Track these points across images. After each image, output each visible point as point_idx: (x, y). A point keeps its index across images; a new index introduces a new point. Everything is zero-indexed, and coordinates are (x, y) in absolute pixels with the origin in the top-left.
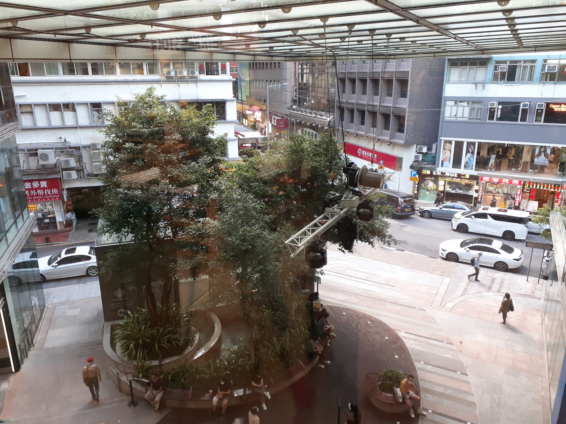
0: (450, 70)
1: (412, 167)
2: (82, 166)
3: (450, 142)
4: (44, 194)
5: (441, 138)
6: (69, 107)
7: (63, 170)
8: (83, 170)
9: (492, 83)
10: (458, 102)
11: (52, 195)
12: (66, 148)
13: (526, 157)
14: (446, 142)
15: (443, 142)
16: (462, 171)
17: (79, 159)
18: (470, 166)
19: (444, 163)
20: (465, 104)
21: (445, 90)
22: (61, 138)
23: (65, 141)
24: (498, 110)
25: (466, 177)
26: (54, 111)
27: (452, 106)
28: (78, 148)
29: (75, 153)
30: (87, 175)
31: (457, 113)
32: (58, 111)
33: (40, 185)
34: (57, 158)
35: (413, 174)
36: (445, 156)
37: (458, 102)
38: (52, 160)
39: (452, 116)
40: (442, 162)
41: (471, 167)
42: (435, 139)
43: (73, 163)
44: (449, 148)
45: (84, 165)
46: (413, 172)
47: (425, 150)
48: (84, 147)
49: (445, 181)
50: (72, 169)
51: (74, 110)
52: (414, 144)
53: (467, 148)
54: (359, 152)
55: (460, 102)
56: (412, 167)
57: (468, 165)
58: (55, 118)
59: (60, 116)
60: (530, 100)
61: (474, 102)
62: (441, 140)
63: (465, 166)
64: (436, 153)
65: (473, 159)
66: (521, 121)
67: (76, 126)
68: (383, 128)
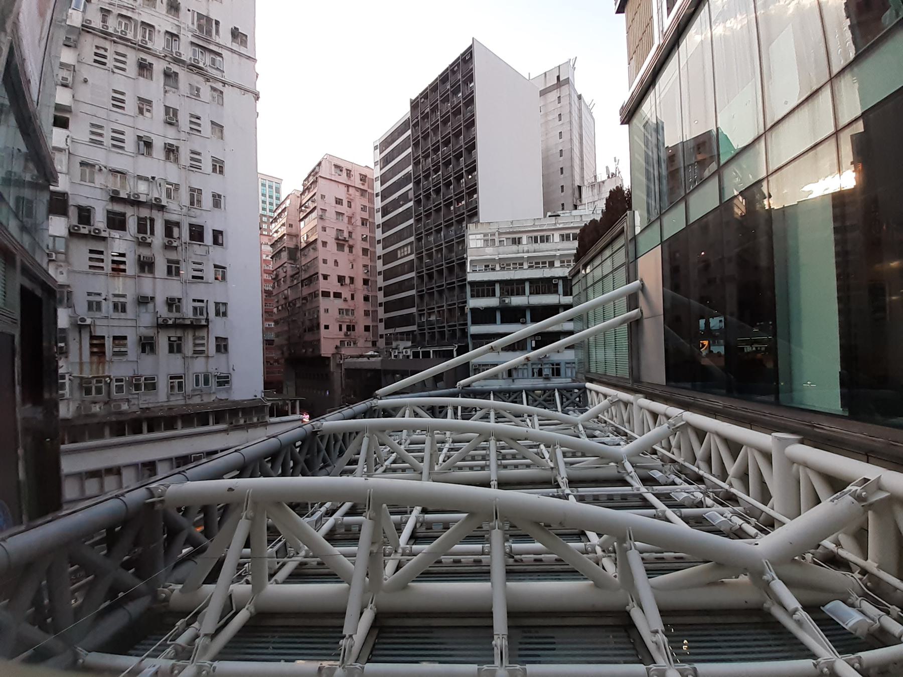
6: (116, 471)
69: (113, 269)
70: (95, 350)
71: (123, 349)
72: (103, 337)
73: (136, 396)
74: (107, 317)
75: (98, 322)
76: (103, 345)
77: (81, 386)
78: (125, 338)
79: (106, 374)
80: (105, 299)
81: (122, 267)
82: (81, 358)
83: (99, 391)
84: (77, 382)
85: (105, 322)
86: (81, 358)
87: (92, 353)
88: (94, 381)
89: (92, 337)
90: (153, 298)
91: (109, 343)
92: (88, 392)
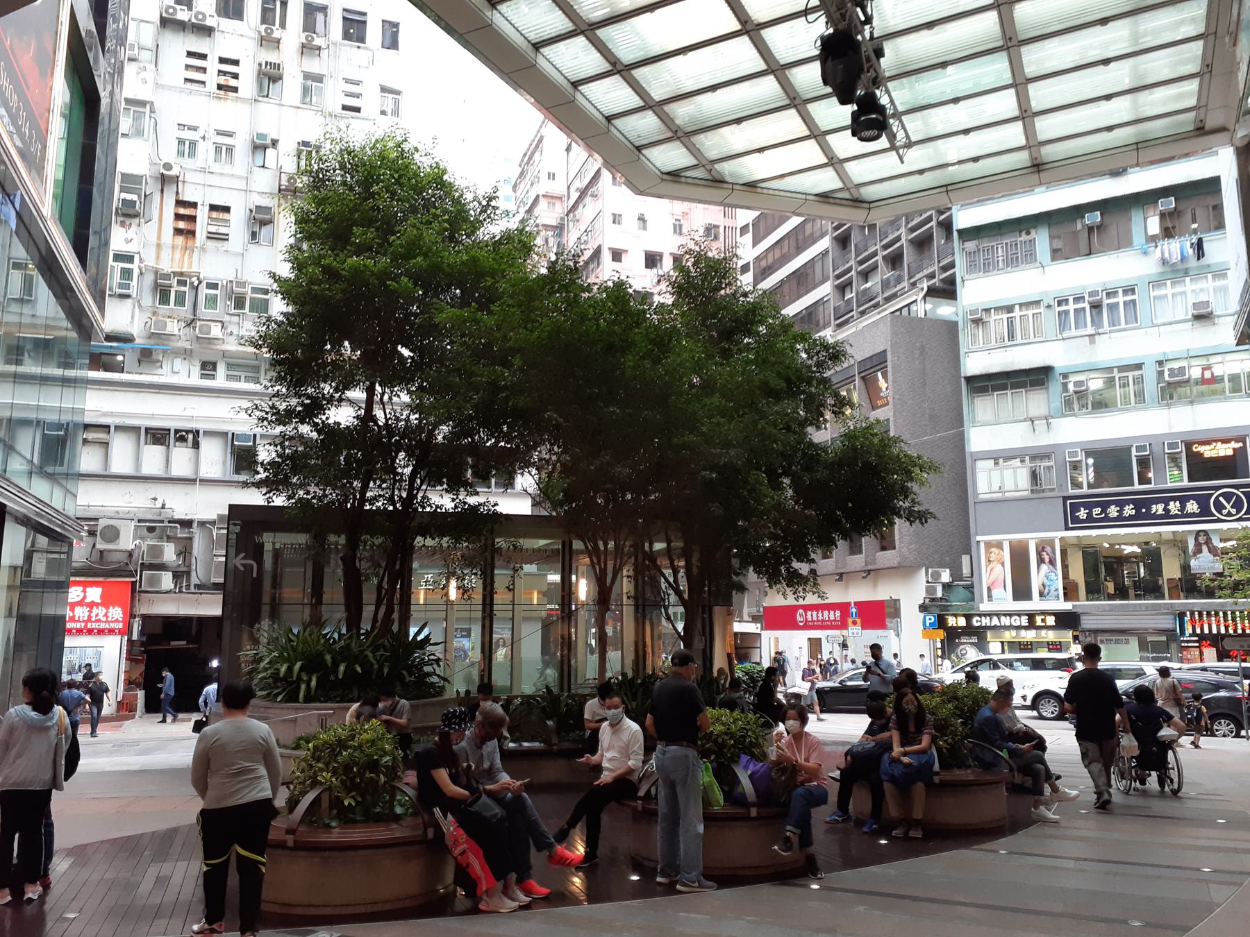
0: (973, 403)
1: (923, 608)
2: (189, 566)
3: (999, 545)
4: (90, 617)
5: (978, 538)
6: (189, 437)
7: (144, 567)
8: (188, 573)
9: (1064, 416)
10: (1001, 460)
11: (107, 622)
12: (162, 521)
13: (1171, 570)
14: (989, 545)
15: (982, 545)
16: (1035, 604)
17: (185, 552)
18: (1052, 591)
19: (994, 593)
20: (1017, 462)
21: (969, 440)
22: (155, 499)
23: (163, 507)
24: (1087, 469)
25: (1048, 624)
26: (154, 444)
27: (990, 470)
28: (187, 524)
29: (181, 533)
30: (196, 586)
31: (1002, 482)
32: (162, 444)
33: (85, 597)
34: (137, 542)
35: (928, 622)
36: (993, 577)
37: (1001, 460)
38: (127, 541)
39: (993, 490)
40: (989, 589)
41: (1056, 593)
42: (967, 547)
43: (169, 553)
44: (999, 557)
45: (193, 561)
46: (927, 618)
47: (946, 576)
48: (202, 524)
49: (1002, 643)
50: (162, 567)
51: (196, 445)
52: (919, 567)
53: (1039, 554)
54: (799, 619)
55: (1006, 459)
56: (923, 608)
57: (1046, 591)
58: (153, 459)
59: (164, 455)
60: (1152, 440)
61: (1033, 458)
62: (978, 542)
63: (1041, 594)
64: (972, 574)
65: (1056, 575)
66: (1140, 484)
67: (194, 477)
68: (847, 553)
69: (220, 87)
70: (182, 225)
71: (222, 230)
72: (194, 205)
73: (236, 319)
74: (203, 170)
75: (189, 177)
76: (193, 219)
77: (156, 286)
78: (226, 209)
79: (194, 269)
80: (204, 138)
81: (232, 83)
82: (159, 237)
83: (180, 299)
84: (149, 279)
85: (200, 178)
86: (159, 237)
87: (178, 231)
88: (174, 282)
89: (180, 203)
90: (274, 143)
91: (202, 214)
92: (164, 299)
